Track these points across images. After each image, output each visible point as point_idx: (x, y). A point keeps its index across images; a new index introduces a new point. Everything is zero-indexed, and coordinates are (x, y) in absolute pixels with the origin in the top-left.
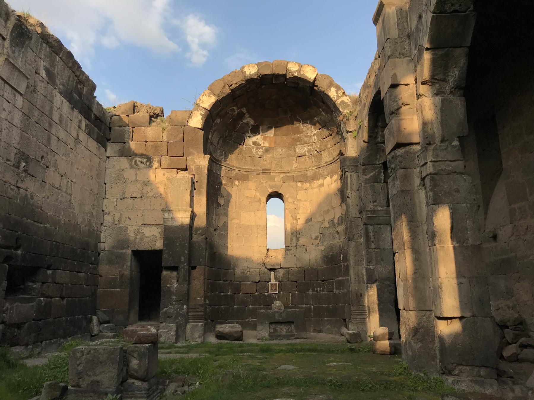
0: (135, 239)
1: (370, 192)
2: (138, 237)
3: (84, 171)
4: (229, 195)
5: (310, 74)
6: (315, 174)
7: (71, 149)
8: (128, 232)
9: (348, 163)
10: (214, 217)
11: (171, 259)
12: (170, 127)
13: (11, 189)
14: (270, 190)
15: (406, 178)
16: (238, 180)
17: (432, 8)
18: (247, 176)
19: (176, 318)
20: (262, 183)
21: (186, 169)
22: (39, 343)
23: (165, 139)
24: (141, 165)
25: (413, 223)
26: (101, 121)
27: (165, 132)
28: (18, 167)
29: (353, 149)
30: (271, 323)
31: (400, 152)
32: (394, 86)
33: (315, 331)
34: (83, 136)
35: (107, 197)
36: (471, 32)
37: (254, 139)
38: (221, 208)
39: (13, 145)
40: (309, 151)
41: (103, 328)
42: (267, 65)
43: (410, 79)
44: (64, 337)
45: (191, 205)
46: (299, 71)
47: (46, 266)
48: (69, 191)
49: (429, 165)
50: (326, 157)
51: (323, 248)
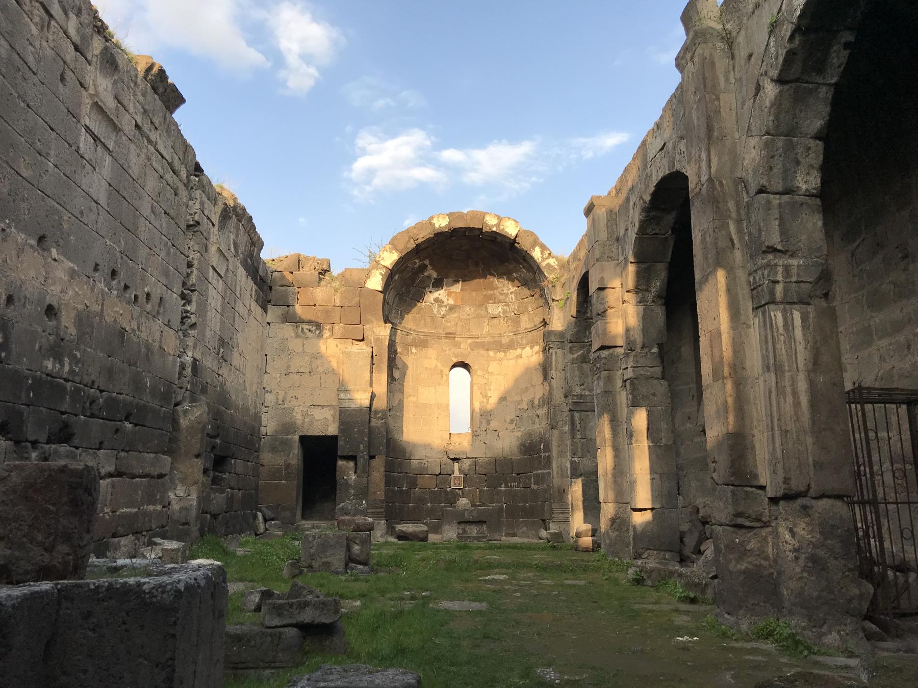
0: (303, 423)
1: (577, 373)
4: (405, 366)
5: (511, 230)
6: (512, 341)
9: (553, 339)
12: (343, 289)
14: (455, 360)
15: (609, 380)
16: (416, 346)
17: (636, 230)
18: (427, 340)
20: (445, 351)
21: (363, 340)
23: (338, 303)
25: (614, 421)
27: (338, 295)
29: (560, 321)
30: (459, 523)
31: (605, 353)
32: (602, 289)
33: (507, 535)
36: (671, 250)
37: (436, 294)
38: (396, 383)
40: (504, 312)
41: (270, 526)
42: (460, 216)
43: (616, 283)
46: (498, 225)
49: (630, 370)
50: (526, 322)
51: (519, 434)
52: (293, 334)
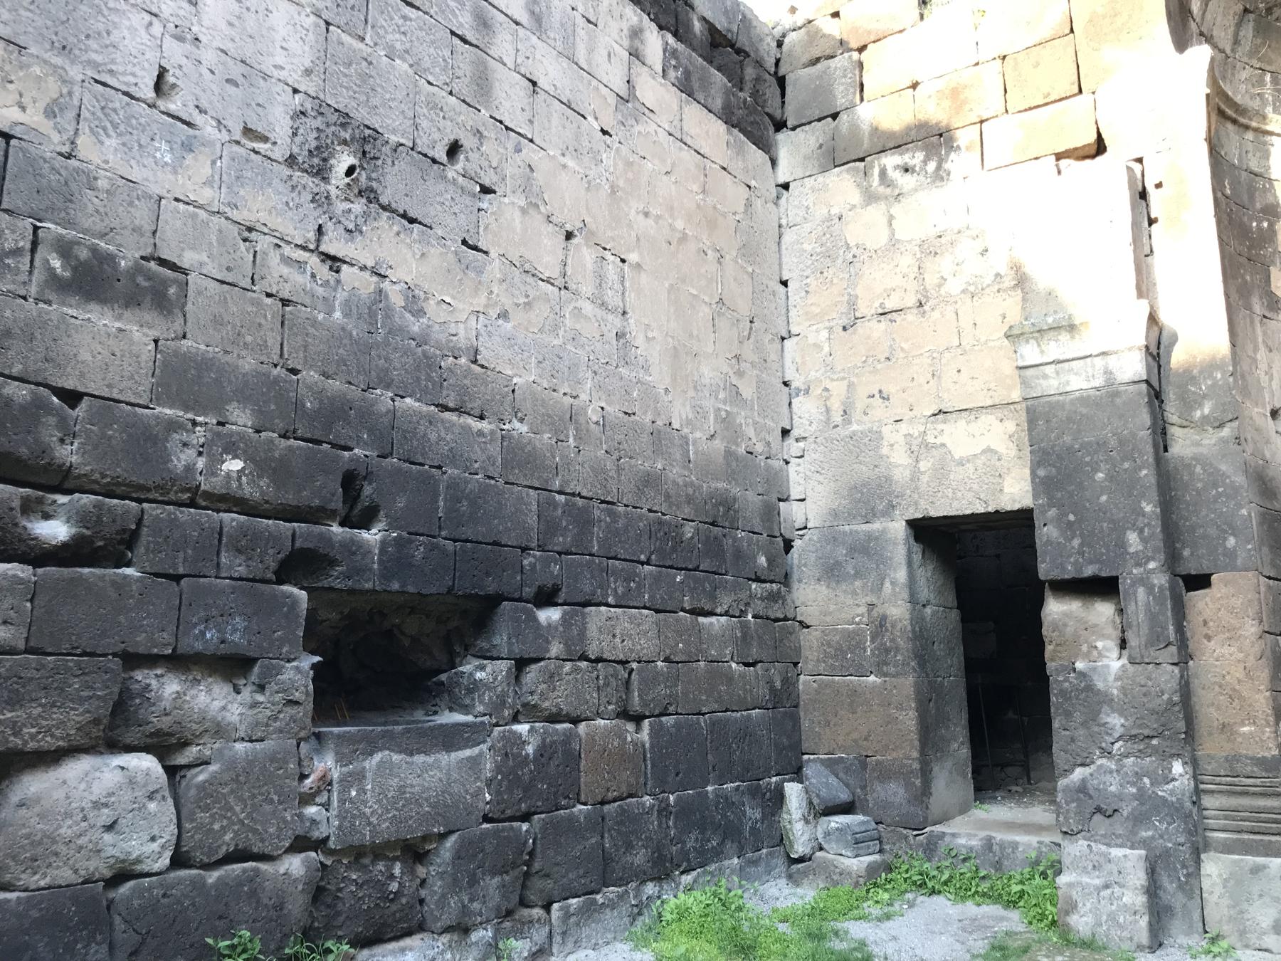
2: (923, 466)
3: (680, 224)
7: (604, 132)
8: (885, 451)
10: (1262, 355)
11: (1076, 542)
13: (287, 260)
19: (1139, 819)
22: (537, 912)
24: (906, 181)
26: (739, 51)
28: (321, 173)
34: (656, 91)
35: (794, 330)
39: (276, 73)
41: (827, 834)
44: (662, 870)
45: (1144, 287)
47: (528, 591)
48: (613, 299)
52: (855, 197)
